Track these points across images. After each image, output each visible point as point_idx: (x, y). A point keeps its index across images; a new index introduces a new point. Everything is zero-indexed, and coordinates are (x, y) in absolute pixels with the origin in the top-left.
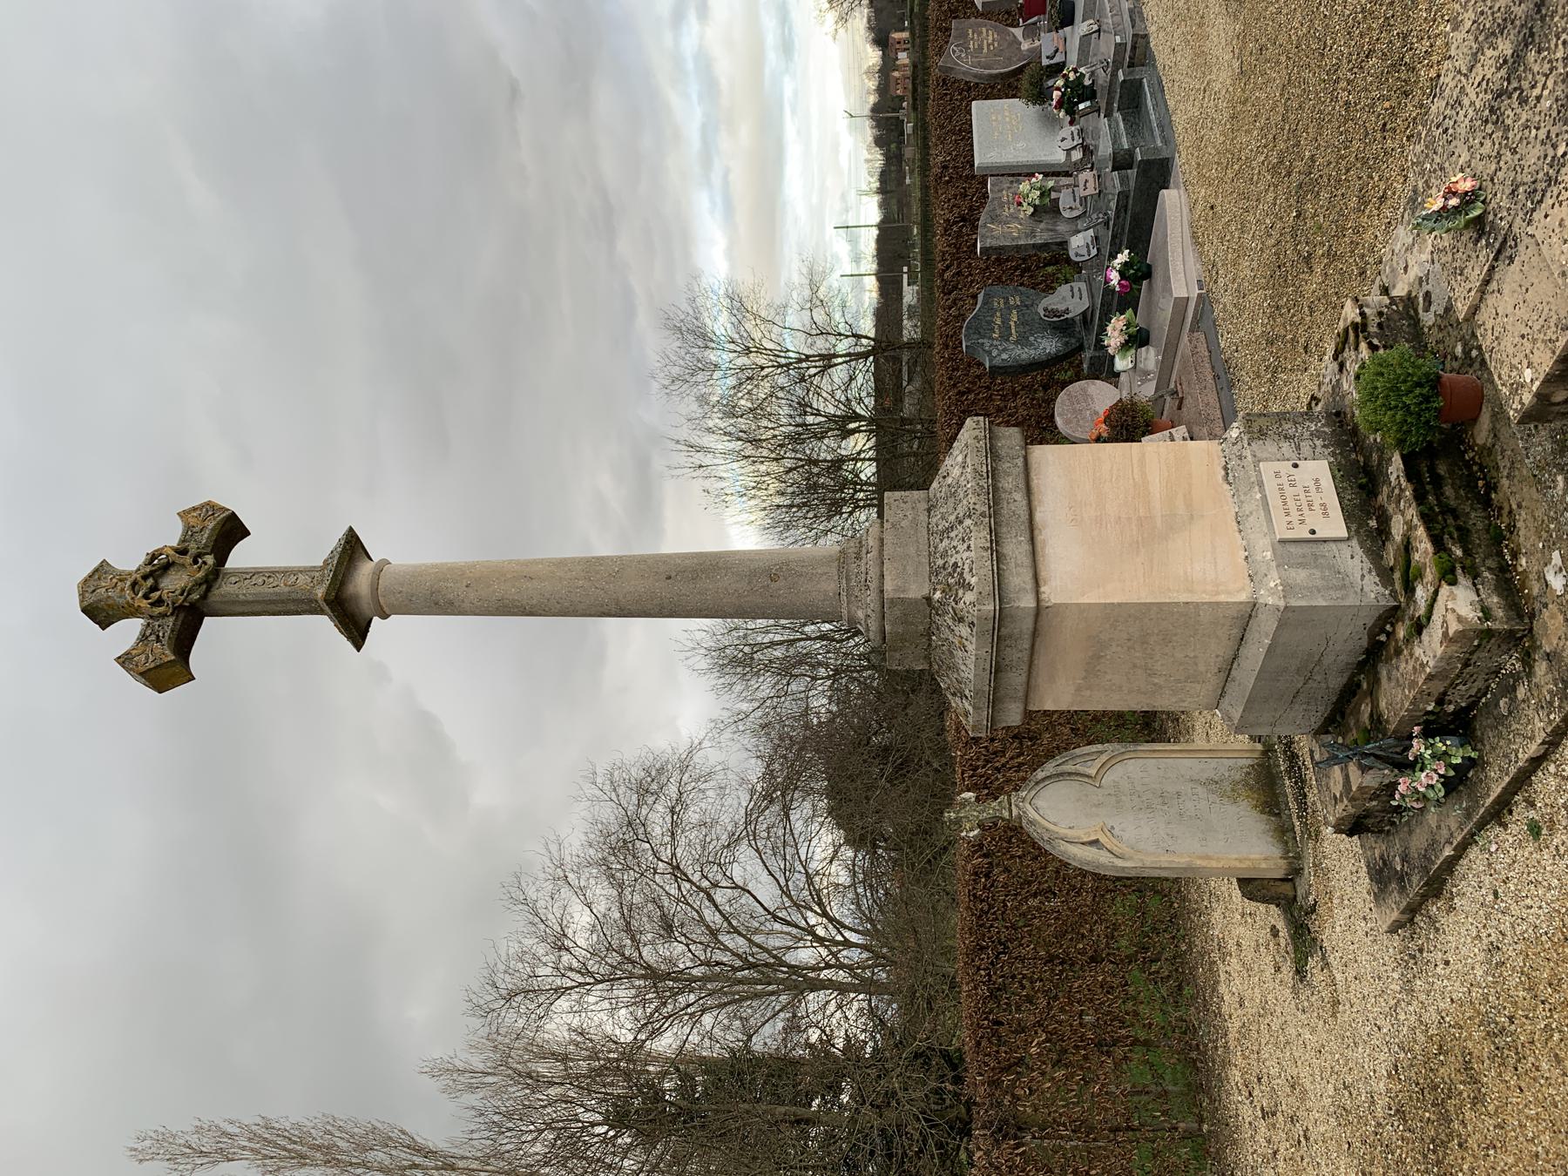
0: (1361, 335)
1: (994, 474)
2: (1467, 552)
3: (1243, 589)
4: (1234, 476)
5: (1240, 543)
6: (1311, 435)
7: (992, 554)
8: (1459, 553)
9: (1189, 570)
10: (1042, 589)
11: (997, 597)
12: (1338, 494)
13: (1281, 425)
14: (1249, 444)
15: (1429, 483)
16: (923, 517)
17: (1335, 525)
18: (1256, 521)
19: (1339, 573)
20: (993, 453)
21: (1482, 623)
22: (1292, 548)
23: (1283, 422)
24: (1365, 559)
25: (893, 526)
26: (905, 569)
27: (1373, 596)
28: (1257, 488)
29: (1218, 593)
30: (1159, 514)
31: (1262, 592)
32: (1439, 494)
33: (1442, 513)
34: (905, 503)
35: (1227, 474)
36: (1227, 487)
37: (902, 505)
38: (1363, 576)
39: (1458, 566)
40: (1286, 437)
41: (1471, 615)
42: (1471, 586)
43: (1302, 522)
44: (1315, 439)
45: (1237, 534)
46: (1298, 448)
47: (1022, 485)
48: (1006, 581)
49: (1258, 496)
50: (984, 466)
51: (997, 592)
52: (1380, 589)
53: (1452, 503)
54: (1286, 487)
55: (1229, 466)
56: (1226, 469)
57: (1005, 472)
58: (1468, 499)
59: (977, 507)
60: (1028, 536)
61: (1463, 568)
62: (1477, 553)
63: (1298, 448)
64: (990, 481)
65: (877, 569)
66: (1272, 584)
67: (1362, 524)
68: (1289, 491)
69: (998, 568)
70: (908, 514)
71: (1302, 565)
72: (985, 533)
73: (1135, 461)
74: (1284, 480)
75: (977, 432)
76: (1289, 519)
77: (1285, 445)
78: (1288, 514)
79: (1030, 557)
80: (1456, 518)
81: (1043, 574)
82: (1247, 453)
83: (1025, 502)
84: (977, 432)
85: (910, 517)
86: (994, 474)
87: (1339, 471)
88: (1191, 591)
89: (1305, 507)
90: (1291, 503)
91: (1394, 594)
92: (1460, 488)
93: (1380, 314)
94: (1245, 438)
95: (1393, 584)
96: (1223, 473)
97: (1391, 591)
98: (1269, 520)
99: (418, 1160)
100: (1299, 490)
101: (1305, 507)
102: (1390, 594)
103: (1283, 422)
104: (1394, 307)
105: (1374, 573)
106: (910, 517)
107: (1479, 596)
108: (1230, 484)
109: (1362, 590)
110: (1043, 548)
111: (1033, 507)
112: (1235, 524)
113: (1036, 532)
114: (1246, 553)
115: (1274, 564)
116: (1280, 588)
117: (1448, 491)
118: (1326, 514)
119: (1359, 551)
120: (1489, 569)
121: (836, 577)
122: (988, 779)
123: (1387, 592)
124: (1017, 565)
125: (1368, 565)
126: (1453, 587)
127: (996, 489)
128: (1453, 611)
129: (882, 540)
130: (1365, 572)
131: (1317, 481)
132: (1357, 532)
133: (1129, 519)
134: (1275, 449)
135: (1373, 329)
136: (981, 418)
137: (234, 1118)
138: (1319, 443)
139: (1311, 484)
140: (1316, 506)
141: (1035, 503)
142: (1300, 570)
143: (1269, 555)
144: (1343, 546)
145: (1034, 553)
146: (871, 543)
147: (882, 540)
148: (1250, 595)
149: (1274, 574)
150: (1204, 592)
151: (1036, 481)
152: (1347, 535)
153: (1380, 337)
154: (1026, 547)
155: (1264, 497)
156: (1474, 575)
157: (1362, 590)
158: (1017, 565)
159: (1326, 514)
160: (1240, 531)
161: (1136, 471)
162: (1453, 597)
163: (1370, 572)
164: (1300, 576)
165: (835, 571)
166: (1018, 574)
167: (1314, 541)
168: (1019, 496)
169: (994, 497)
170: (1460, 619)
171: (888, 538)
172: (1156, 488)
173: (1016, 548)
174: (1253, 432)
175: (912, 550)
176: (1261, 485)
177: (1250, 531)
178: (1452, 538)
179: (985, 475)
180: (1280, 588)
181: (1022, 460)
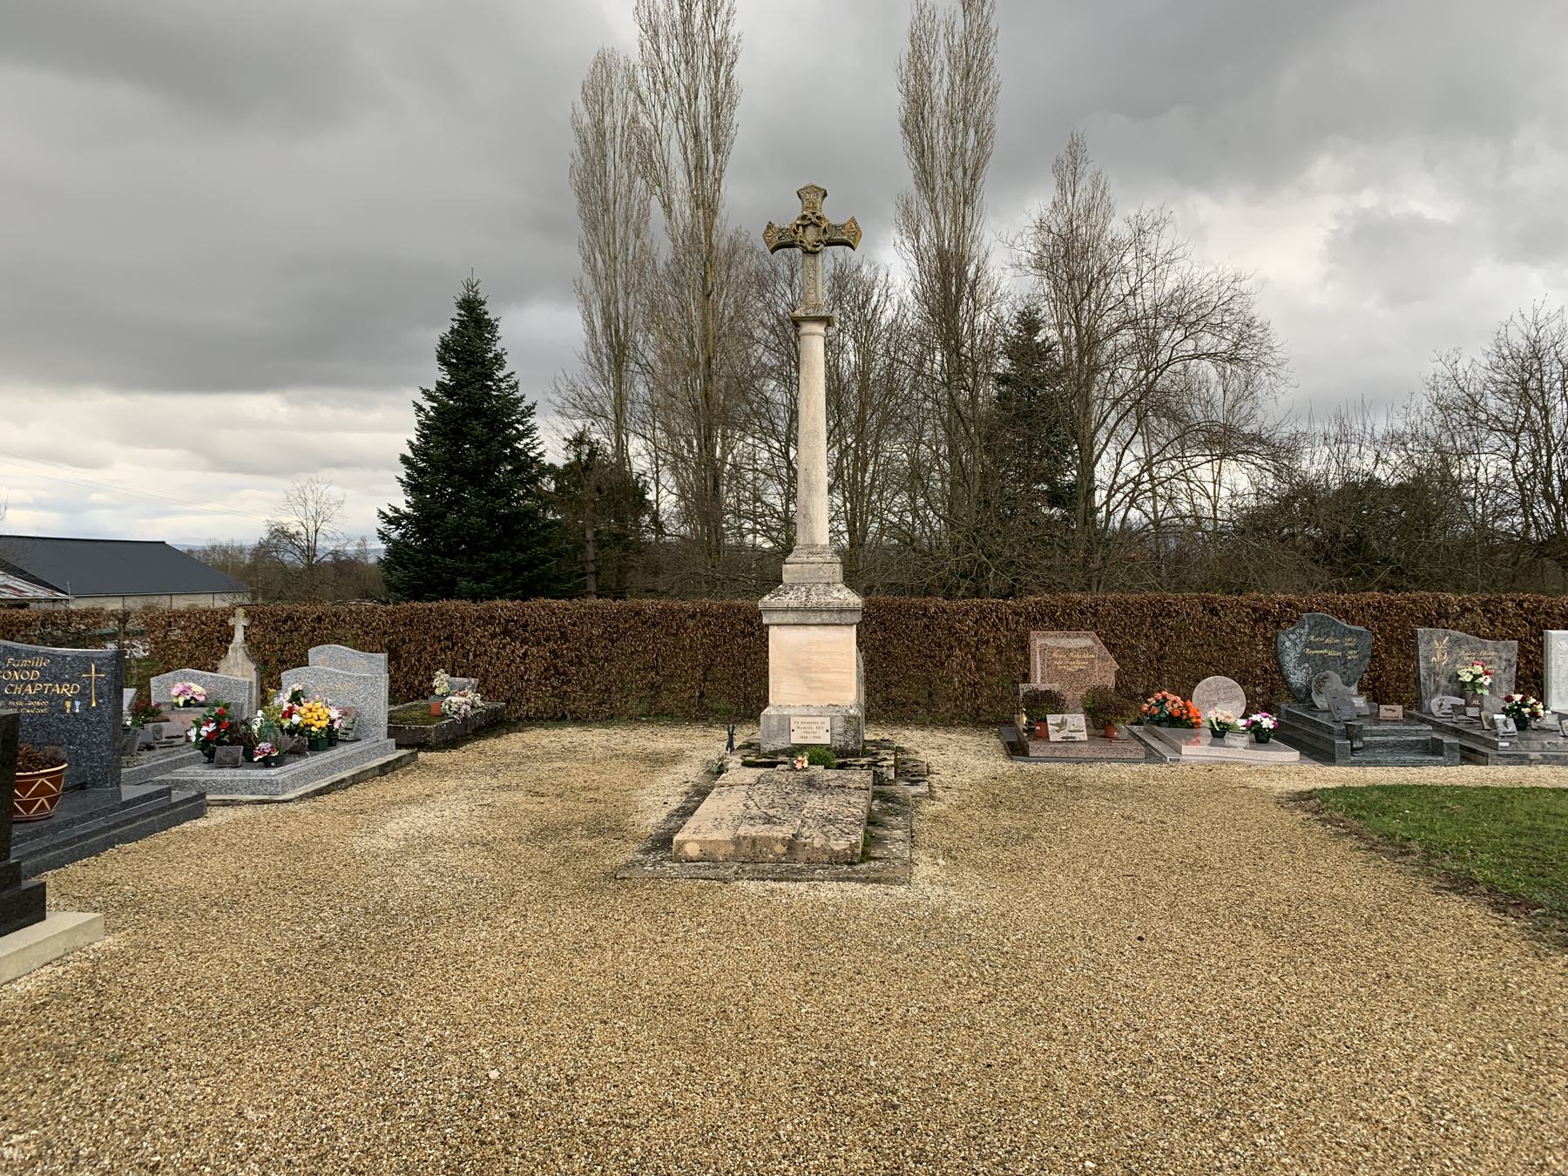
1: (829, 610)
16: (824, 581)
17: (796, 739)
20: (841, 611)
68: (814, 726)
71: (779, 724)
81: (783, 628)
86: (829, 610)
90: (806, 725)
99: (969, 173)
119: (786, 746)
125: (779, 748)
127: (822, 611)
134: (839, 724)
137: (996, 6)
138: (842, 743)
149: (777, 713)
162: (737, 763)
164: (774, 722)
167: (790, 731)
168: (818, 620)
169: (818, 610)
171: (813, 566)
172: (825, 676)
173: (791, 617)
175: (807, 576)
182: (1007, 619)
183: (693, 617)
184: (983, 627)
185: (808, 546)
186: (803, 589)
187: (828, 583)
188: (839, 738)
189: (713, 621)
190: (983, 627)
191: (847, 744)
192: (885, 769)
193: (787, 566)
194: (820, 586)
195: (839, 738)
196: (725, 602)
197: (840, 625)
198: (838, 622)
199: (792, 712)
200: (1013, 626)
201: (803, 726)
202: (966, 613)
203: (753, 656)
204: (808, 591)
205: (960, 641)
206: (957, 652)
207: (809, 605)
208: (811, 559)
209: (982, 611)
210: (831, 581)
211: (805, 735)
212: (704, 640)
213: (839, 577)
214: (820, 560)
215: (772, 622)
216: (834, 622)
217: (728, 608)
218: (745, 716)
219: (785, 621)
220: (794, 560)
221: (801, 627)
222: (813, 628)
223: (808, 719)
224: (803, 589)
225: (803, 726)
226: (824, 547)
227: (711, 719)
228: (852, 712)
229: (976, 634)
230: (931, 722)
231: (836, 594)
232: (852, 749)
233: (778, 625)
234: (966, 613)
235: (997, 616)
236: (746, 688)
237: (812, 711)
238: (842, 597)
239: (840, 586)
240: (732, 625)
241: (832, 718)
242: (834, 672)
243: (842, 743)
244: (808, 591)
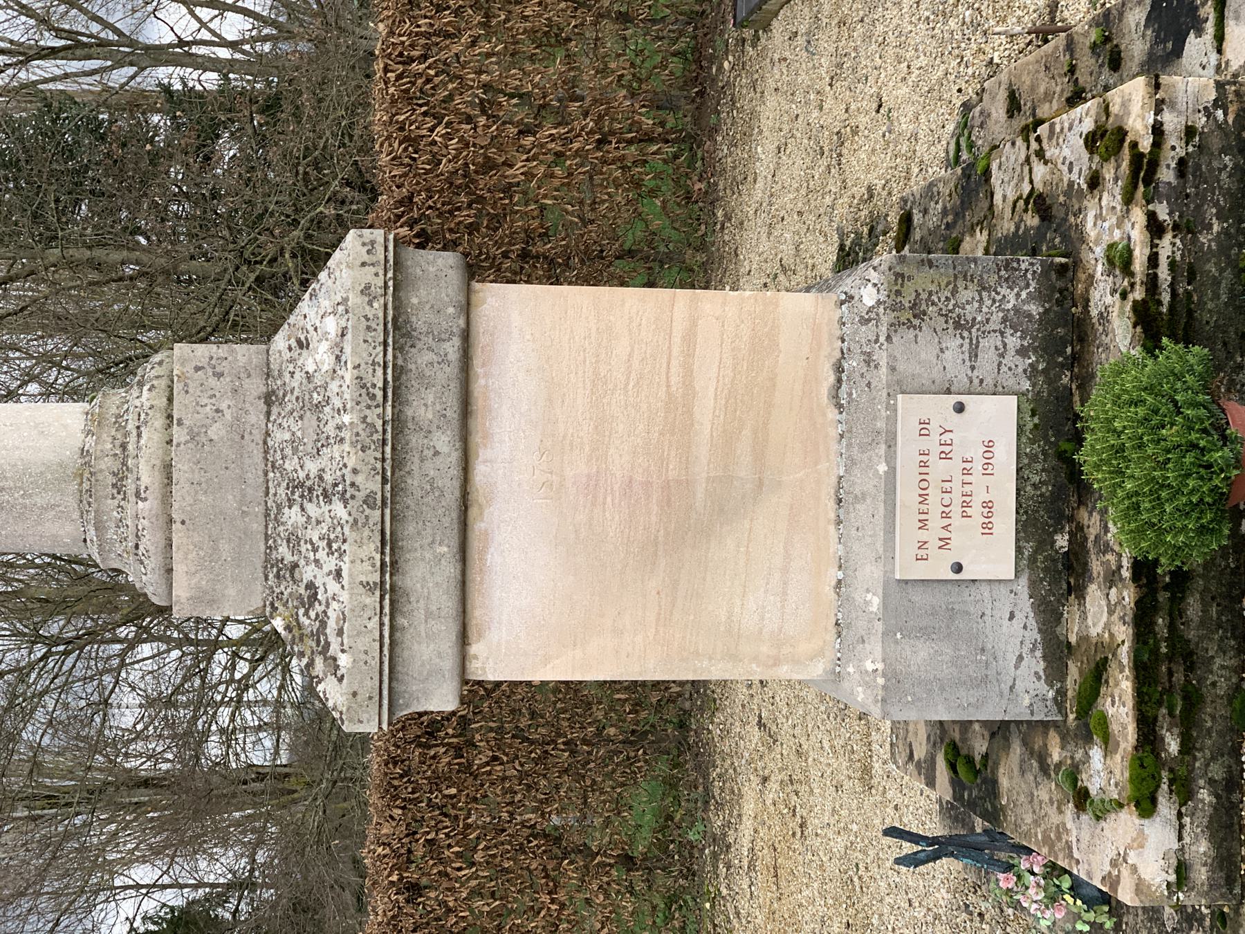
0: (1141, 188)
2: (1187, 747)
3: (821, 653)
4: (850, 394)
5: (836, 549)
6: (1004, 320)
7: (382, 598)
8: (1173, 746)
9: (737, 610)
10: (474, 649)
11: (385, 702)
12: (1019, 470)
13: (955, 292)
14: (889, 338)
15: (1166, 587)
16: (255, 416)
18: (866, 513)
19: (983, 650)
21: (1171, 893)
22: (919, 597)
23: (961, 284)
24: (1032, 623)
25: (193, 436)
26: (215, 549)
27: (1027, 702)
28: (883, 447)
29: (777, 662)
30: (704, 475)
31: (851, 669)
32: (1176, 613)
33: (1170, 658)
34: (219, 375)
35: (839, 381)
36: (832, 414)
37: (212, 381)
38: (1020, 658)
39: (1165, 775)
40: (957, 325)
41: (1158, 880)
42: (1174, 818)
43: (945, 543)
44: (1009, 331)
45: (832, 528)
46: (974, 354)
47: (453, 414)
48: (406, 654)
49: (882, 468)
50: (380, 372)
51: (385, 692)
52: (1042, 687)
53: (1192, 635)
54: (933, 459)
55: (846, 366)
56: (839, 369)
57: (421, 376)
58: (1219, 626)
59: (359, 479)
60: (455, 542)
61: (1171, 782)
62: (1201, 750)
63: (974, 354)
64: (389, 410)
65: (160, 537)
66: (870, 666)
67: (1045, 542)
68: (939, 469)
69: (392, 627)
70: (223, 406)
71: (926, 633)
72: (371, 548)
73: (677, 339)
74: (933, 443)
75: (367, 275)
76: (923, 534)
77: (953, 343)
78: (923, 524)
79: (455, 593)
80: (1190, 668)
81: (477, 614)
82: (882, 357)
83: (455, 456)
84: (367, 275)
85: (228, 417)
87: (1033, 415)
88: (734, 657)
89: (956, 510)
90: (934, 496)
91: (1060, 700)
92: (1213, 598)
93: (1190, 132)
94: (886, 320)
95: (1063, 676)
96: (832, 379)
97: (1058, 692)
98: (890, 530)
100: (956, 466)
101: (956, 510)
102: (1055, 699)
103: (961, 284)
104: (1220, 114)
105: (1039, 654)
106: (228, 417)
107: (1180, 838)
108: (839, 406)
109: (1012, 688)
110: (484, 551)
111: (472, 445)
112: (832, 504)
113: (473, 512)
114: (840, 575)
115: (879, 627)
116: (881, 681)
117: (1193, 607)
118: (987, 528)
119: (1025, 604)
120: (1211, 782)
121: (76, 515)
122: (428, 81)
123: (1051, 694)
124: (429, 615)
125: (1034, 635)
126: (1146, 822)
127: (398, 424)
128: (1134, 869)
129: (168, 469)
130: (1025, 650)
131: (989, 445)
132: (1032, 560)
133: (647, 485)
135: (1167, 175)
136: (378, 234)
138: (1013, 342)
139: (977, 453)
140: (976, 510)
141: (476, 439)
142: (919, 644)
143: (875, 602)
144: (1004, 590)
145: (464, 573)
146: (145, 480)
147: (168, 468)
148: (829, 667)
150: (755, 659)
151: (482, 382)
152: (1013, 577)
153: (1177, 197)
154: (450, 569)
155: (892, 471)
156: (1184, 792)
157: (1012, 688)
158: (429, 615)
159: (987, 528)
160: (839, 522)
161: (674, 363)
162: (1140, 841)
163: (1032, 651)
165: (72, 502)
166: (430, 637)
168: (445, 441)
170: (1140, 887)
174: (902, 308)
175: (230, 502)
176: (891, 444)
177: (853, 532)
178: (1171, 714)
179: (379, 394)
180: (881, 681)
181: (457, 341)
182: (427, 35)
183: (414, 890)
184: (450, 97)
185: (86, 496)
186: (293, 516)
187: (269, 399)
188: (987, 357)
189: (425, 833)
190: (450, 97)
191: (1014, 320)
192: (1171, 121)
193: (181, 591)
194: (280, 436)
195: (987, 357)
196: (374, 798)
197: (466, 336)
198: (452, 348)
199: (869, 574)
200: (448, 17)
201: (935, 522)
202: (411, 141)
203: (524, 722)
204: (303, 490)
205: (488, 166)
206: (515, 173)
207: (375, 485)
208: (147, 475)
209: (406, 97)
210: (256, 386)
211: (976, 510)
212: (479, 857)
213: (243, 354)
214: (151, 438)
215: (448, 663)
216: (452, 370)
217: (390, 792)
218: (682, 745)
219: (446, 603)
220: (153, 563)
221: (478, 527)
222: (481, 472)
223: (907, 494)
224: (293, 516)
225: (935, 522)
226: (95, 424)
227: (692, 836)
228: (869, 297)
229: (469, 119)
230: (702, 246)
231: (320, 357)
232: (1039, 296)
233: (464, 639)
234: (411, 141)
235: (424, 57)
236: (609, 740)
237: (866, 482)
238: (331, 326)
239: (280, 341)
240: (436, 782)
241: (901, 386)
242: (688, 373)
243: (1013, 342)
244: (303, 490)
